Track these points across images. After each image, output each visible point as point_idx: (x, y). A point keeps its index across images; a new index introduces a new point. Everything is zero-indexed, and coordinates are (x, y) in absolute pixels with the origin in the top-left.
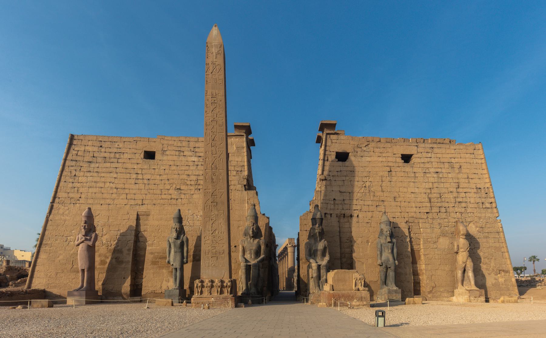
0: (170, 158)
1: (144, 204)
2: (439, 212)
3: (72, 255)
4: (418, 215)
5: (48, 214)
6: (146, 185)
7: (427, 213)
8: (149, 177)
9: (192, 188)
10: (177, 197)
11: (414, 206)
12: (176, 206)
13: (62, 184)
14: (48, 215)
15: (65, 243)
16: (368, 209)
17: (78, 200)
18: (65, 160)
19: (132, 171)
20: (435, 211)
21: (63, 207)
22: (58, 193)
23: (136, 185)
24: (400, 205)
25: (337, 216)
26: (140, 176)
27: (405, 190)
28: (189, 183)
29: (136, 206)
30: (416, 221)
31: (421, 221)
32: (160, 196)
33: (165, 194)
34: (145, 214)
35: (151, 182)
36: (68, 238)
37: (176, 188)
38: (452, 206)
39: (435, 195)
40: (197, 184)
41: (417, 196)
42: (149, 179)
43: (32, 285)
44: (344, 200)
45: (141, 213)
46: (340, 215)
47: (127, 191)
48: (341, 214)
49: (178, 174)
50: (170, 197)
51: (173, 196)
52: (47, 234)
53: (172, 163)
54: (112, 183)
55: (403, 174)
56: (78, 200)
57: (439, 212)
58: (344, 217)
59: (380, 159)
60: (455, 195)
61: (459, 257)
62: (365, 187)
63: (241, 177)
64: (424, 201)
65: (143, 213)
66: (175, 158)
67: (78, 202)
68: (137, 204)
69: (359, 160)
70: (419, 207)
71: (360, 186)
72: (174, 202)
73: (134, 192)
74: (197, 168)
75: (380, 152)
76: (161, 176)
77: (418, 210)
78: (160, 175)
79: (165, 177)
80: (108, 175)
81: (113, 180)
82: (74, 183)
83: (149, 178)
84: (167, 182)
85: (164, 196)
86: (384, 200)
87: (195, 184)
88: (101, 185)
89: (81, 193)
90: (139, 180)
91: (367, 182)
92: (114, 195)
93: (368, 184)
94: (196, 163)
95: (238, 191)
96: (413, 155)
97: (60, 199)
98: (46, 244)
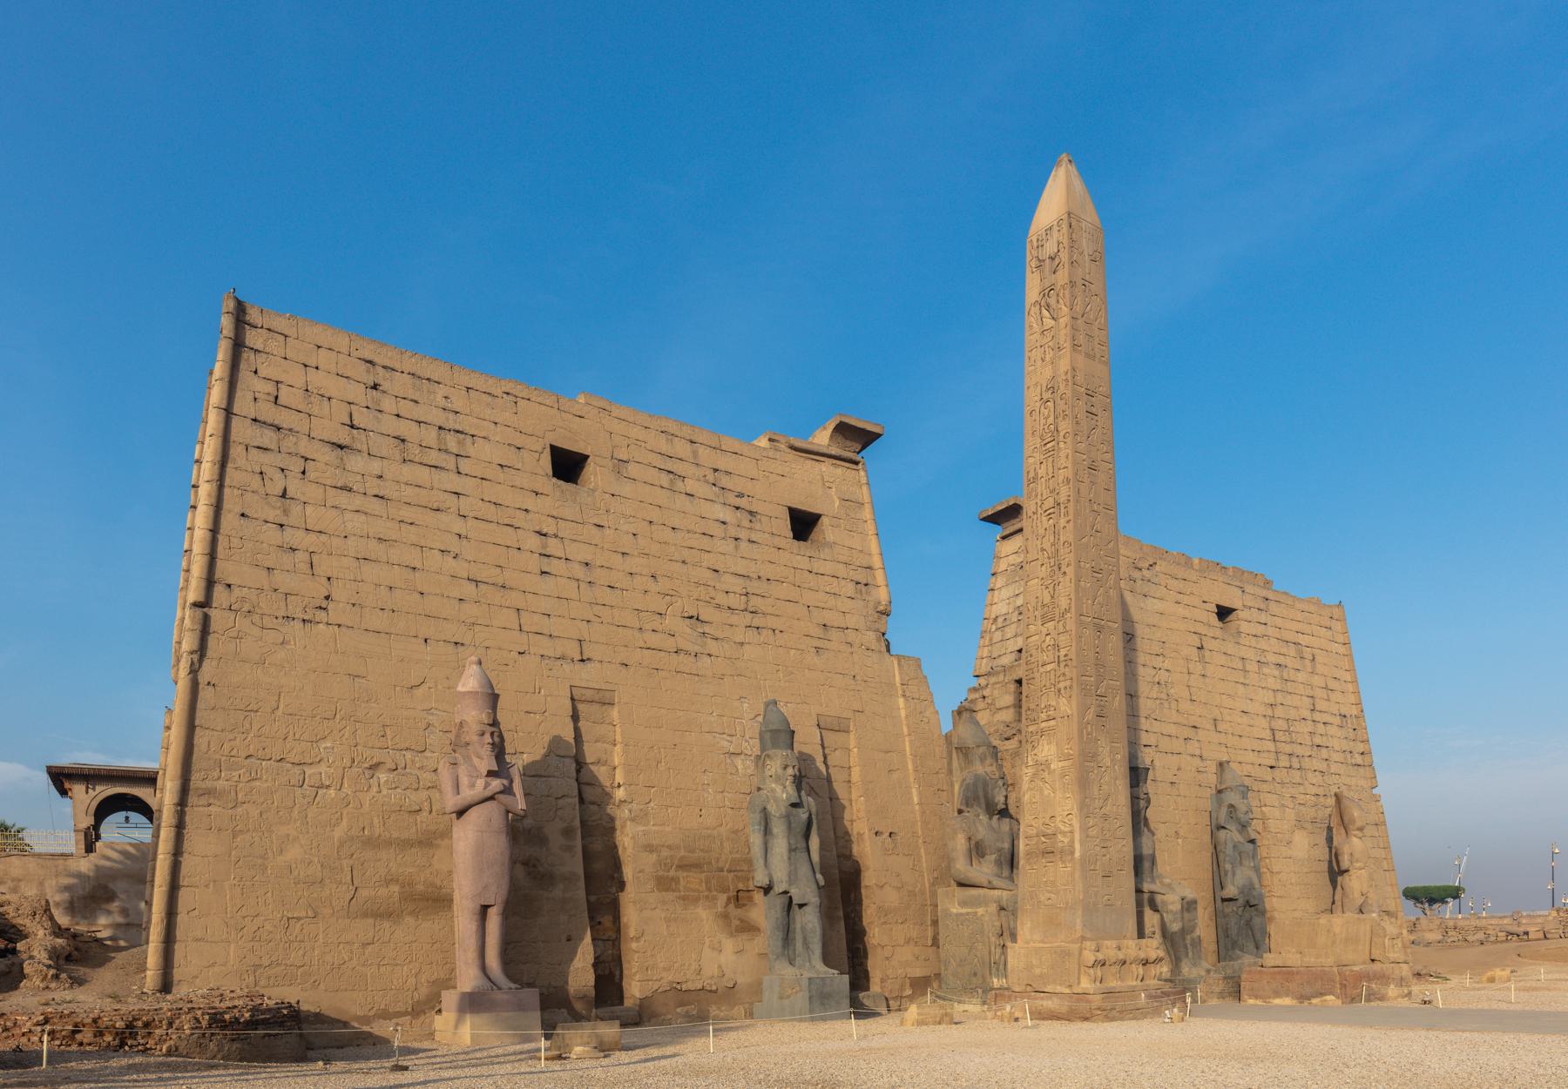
1: (588, 659)
3: (342, 844)
5: (196, 657)
6: (583, 585)
7: (1271, 767)
8: (583, 553)
9: (734, 619)
10: (697, 649)
12: (696, 678)
14: (196, 660)
15: (299, 791)
17: (321, 608)
19: (520, 518)
21: (256, 631)
22: (220, 564)
23: (547, 577)
26: (553, 546)
28: (721, 599)
29: (561, 662)
32: (637, 634)
33: (653, 631)
34: (596, 698)
35: (601, 576)
36: (309, 771)
37: (686, 615)
39: (1280, 721)
40: (746, 610)
41: (1252, 722)
42: (587, 564)
43: (175, 971)
45: (584, 691)
47: (515, 599)
49: (683, 562)
50: (670, 644)
51: (683, 645)
52: (204, 747)
53: (654, 514)
54: (452, 554)
56: (321, 608)
59: (1180, 610)
61: (1350, 880)
62: (1158, 683)
63: (871, 604)
65: (589, 694)
66: (662, 497)
67: (321, 615)
68: (562, 658)
69: (1142, 605)
71: (1149, 680)
72: (685, 662)
73: (545, 605)
74: (736, 547)
75: (1178, 590)
76: (628, 558)
78: (623, 554)
79: (635, 563)
80: (431, 518)
81: (454, 545)
82: (288, 531)
83: (588, 558)
84: (653, 587)
85: (654, 640)
87: (742, 607)
88: (413, 558)
89: (329, 579)
90: (555, 561)
91: (1160, 669)
92: (470, 610)
93: (1163, 676)
94: (733, 532)
95: (870, 653)
96: (1235, 610)
97: (237, 592)
98: (209, 792)
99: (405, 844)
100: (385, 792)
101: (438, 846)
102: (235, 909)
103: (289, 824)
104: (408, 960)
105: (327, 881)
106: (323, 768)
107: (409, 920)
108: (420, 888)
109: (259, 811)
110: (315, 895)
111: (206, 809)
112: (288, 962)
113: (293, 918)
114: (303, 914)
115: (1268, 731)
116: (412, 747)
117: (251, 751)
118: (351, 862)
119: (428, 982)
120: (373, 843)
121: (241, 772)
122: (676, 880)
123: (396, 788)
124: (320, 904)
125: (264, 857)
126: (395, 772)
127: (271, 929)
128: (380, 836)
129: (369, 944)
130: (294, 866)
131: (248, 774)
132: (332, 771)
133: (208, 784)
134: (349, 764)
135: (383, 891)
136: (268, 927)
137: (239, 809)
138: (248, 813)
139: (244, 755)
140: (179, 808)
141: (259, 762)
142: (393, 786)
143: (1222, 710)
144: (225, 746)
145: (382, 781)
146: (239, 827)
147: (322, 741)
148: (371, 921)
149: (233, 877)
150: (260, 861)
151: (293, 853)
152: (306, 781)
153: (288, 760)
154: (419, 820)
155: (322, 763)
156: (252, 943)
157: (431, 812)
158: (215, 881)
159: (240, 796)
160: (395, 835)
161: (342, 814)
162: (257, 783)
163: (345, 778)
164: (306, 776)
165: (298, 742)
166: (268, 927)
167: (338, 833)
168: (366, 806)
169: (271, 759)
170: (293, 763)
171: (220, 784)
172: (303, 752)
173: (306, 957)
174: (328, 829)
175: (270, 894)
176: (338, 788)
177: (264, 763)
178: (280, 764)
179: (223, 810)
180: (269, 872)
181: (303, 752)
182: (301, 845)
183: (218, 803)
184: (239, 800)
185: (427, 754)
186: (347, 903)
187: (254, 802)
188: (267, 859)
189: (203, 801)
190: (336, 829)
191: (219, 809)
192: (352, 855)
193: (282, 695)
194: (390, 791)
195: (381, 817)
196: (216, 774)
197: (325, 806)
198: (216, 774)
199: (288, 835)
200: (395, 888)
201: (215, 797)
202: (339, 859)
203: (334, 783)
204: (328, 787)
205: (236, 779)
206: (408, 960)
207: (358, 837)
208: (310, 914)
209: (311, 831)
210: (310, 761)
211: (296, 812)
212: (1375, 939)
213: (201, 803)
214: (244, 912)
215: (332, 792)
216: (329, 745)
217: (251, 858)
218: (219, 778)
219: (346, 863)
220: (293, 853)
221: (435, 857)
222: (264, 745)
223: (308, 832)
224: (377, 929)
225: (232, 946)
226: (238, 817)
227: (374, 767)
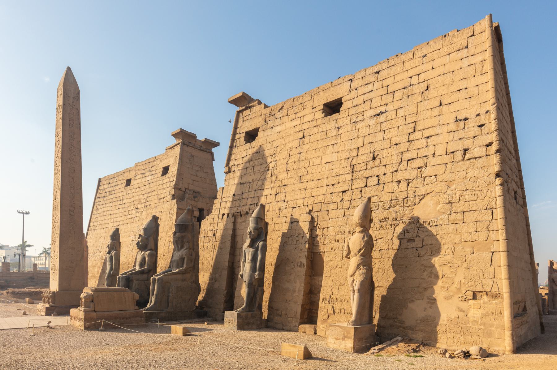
0: (139, 181)
2: (366, 186)
4: (329, 198)
9: (143, 205)
11: (325, 184)
13: (93, 216)
16: (265, 201)
18: (95, 198)
20: (357, 186)
24: (305, 187)
25: (233, 217)
27: (318, 161)
30: (324, 208)
31: (331, 207)
38: (391, 171)
44: (243, 193)
46: (236, 214)
48: (238, 213)
55: (319, 136)
57: (366, 186)
58: (241, 216)
60: (403, 148)
64: (343, 173)
70: (333, 185)
77: (330, 189)
86: (286, 184)
91: (271, 162)
115: (348, 168)
143: (308, 169)
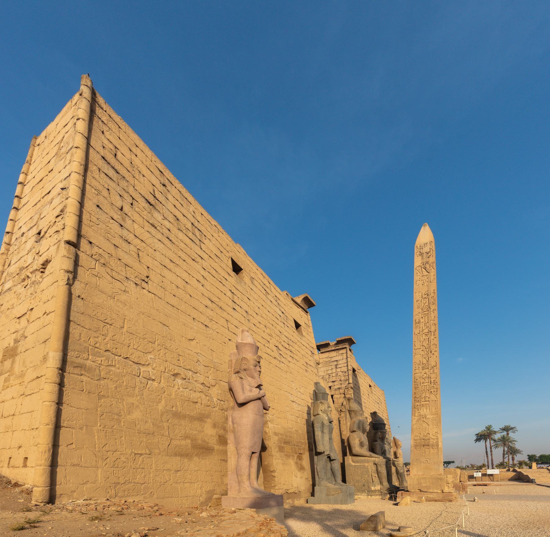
15: (138, 379)
36: (143, 369)
99: (192, 419)
100: (181, 389)
101: (206, 422)
102: (101, 446)
103: (133, 397)
104: (196, 481)
105: (156, 434)
106: (150, 369)
107: (196, 459)
108: (200, 442)
109: (115, 385)
110: (150, 441)
111: (80, 377)
112: (136, 481)
113: (138, 454)
114: (143, 452)
116: (192, 370)
117: (108, 347)
118: (168, 424)
119: (206, 492)
120: (177, 415)
121: (103, 359)
122: (283, 448)
123: (186, 388)
124: (153, 447)
125: (119, 414)
126: (185, 380)
127: (125, 460)
128: (180, 412)
129: (178, 471)
130: (137, 422)
131: (107, 361)
132: (155, 372)
133: (80, 361)
134: (163, 370)
135: (183, 442)
136: (123, 459)
137: (102, 382)
138: (108, 386)
139: (104, 349)
140: (60, 372)
141: (113, 355)
142: (185, 387)
144: (91, 339)
145: (179, 384)
146: (102, 393)
147: (149, 354)
148: (179, 458)
149: (99, 425)
150: (116, 417)
151: (136, 415)
152: (141, 375)
153: (130, 359)
154: (197, 407)
155: (150, 366)
156: (112, 469)
157: (202, 404)
158: (87, 426)
159: (102, 374)
160: (187, 413)
161: (161, 397)
162: (113, 368)
163: (162, 378)
164: (141, 371)
165: (136, 351)
166: (123, 459)
167: (160, 407)
168: (173, 396)
169: (120, 356)
170: (133, 362)
171: (89, 363)
172: (139, 357)
173: (146, 479)
174: (155, 404)
175: (123, 438)
176: (159, 382)
177: (116, 357)
178: (125, 360)
179: (91, 380)
180: (122, 424)
181: (139, 357)
182: (141, 410)
183: (88, 375)
184: (102, 376)
185: (198, 374)
186: (166, 447)
187: (112, 380)
188: (121, 416)
189: (77, 371)
190: (159, 404)
191: (89, 379)
192: (168, 420)
193: (126, 321)
194: (184, 390)
195: (181, 402)
196: (85, 356)
197: (153, 391)
198: (85, 356)
199: (133, 404)
200: (189, 441)
201: (85, 371)
202: (162, 422)
203: (157, 379)
204: (154, 380)
205: (99, 362)
206: (196, 481)
207: (170, 411)
208: (148, 452)
209: (146, 403)
210: (143, 363)
211: (137, 391)
212: (461, 475)
213: (76, 372)
214: (107, 448)
215: (155, 384)
216: (153, 357)
217: (110, 414)
218: (88, 359)
219: (165, 424)
220: (136, 415)
221: (205, 427)
222: (117, 346)
223: (144, 404)
224: (182, 462)
225: (100, 470)
226: (101, 386)
227: (176, 375)
